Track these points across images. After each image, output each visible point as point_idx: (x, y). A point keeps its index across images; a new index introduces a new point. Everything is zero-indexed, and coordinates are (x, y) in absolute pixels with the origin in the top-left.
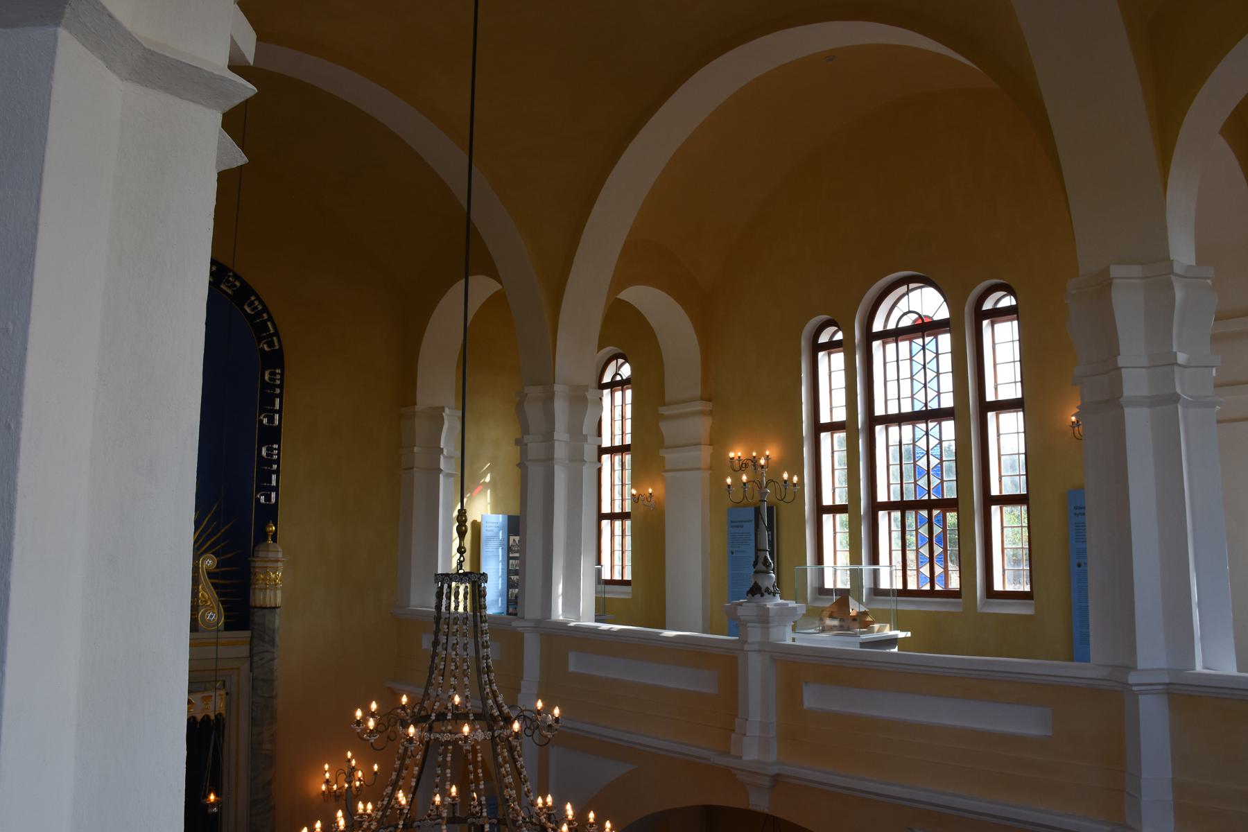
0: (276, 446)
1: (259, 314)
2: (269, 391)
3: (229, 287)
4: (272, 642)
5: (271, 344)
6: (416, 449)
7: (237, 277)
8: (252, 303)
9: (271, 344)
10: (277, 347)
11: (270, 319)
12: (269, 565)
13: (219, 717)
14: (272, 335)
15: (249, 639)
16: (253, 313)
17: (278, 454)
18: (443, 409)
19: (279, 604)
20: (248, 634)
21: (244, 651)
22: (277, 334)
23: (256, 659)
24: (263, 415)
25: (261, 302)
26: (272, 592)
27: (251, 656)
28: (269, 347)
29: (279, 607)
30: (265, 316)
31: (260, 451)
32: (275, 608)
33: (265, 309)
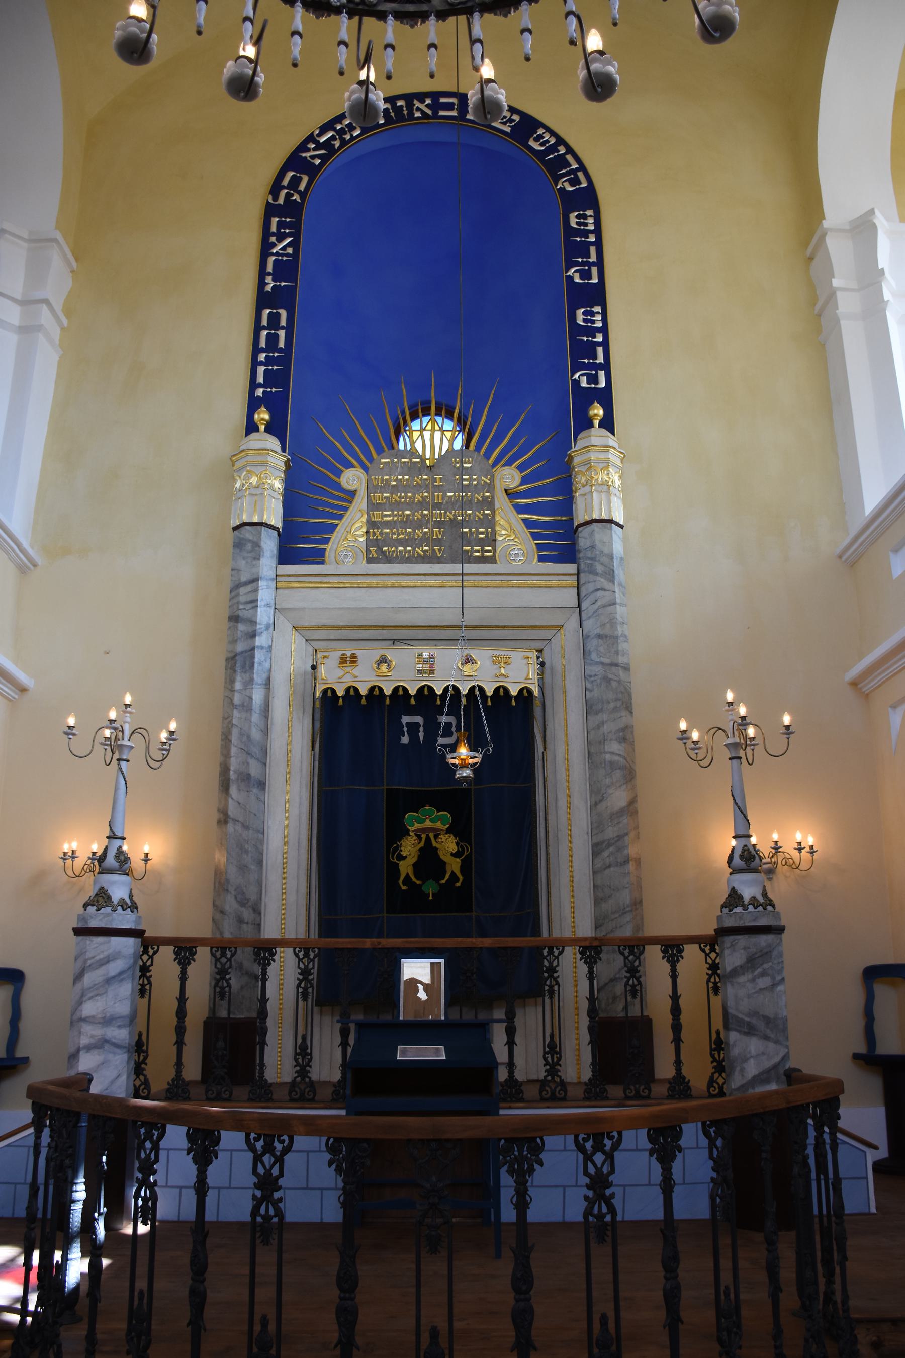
0: (597, 309)
1: (553, 149)
2: (578, 239)
3: (505, 123)
4: (610, 575)
5: (575, 181)
6: (836, 282)
7: (512, 110)
8: (541, 136)
9: (575, 181)
10: (584, 184)
11: (570, 150)
12: (593, 456)
13: (525, 696)
14: (574, 171)
15: (574, 580)
16: (543, 148)
17: (605, 320)
18: (872, 212)
19: (619, 517)
20: (571, 568)
21: (569, 597)
22: (582, 168)
23: (584, 605)
24: (573, 270)
25: (553, 133)
26: (603, 496)
27: (579, 606)
28: (572, 185)
29: (621, 527)
30: (562, 150)
31: (573, 317)
32: (611, 521)
33: (560, 141)
